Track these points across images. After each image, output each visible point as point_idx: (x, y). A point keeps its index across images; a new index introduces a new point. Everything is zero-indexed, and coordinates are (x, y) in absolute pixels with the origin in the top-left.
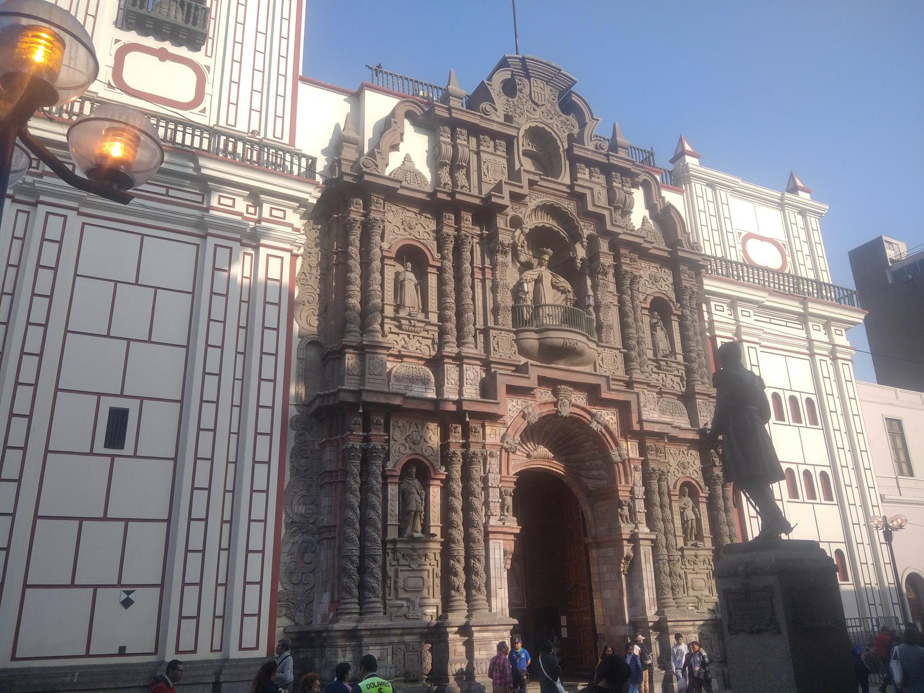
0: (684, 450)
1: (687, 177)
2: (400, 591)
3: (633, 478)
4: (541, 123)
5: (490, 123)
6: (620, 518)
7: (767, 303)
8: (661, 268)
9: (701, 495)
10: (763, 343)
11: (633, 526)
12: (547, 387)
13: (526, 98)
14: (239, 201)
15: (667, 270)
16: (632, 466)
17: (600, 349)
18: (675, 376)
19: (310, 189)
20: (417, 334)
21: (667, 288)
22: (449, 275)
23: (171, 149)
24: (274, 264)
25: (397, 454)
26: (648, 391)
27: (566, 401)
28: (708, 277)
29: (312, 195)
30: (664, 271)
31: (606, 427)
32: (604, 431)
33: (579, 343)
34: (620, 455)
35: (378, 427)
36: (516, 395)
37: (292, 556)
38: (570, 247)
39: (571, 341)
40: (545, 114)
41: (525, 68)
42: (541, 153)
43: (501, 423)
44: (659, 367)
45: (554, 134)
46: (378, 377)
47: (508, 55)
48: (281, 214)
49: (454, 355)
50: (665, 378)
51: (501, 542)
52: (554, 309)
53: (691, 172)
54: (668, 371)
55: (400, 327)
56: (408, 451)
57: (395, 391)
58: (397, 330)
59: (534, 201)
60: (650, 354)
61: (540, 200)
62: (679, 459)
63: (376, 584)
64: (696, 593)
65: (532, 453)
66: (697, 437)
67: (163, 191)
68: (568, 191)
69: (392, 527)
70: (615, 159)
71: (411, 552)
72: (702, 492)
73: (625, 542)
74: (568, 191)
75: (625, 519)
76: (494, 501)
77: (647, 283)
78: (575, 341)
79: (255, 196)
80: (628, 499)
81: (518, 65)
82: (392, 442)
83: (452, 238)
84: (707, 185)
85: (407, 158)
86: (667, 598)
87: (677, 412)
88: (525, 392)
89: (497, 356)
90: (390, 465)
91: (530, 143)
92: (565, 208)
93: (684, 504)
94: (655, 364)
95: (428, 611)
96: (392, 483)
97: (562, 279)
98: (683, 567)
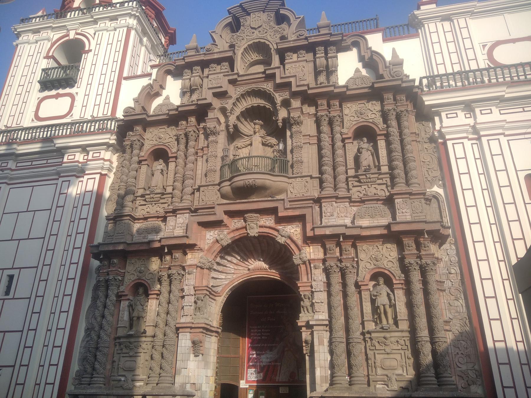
0: (378, 245)
1: (421, 22)
2: (120, 370)
3: (313, 276)
4: (257, 39)
5: (212, 55)
6: (302, 309)
7: (507, 96)
8: (368, 102)
9: (395, 282)
10: (507, 133)
11: (312, 314)
12: (238, 217)
13: (248, 28)
14: (78, 154)
15: (374, 102)
16: (312, 265)
17: (290, 181)
18: (379, 184)
19: (108, 136)
20: (157, 202)
21: (373, 116)
22: (180, 161)
23: (42, 140)
24: (91, 182)
25: (129, 281)
26: (336, 202)
27: (252, 224)
28: (425, 94)
29: (112, 139)
30: (372, 104)
31: (290, 238)
32: (289, 241)
33: (257, 180)
34: (300, 259)
35: (114, 265)
36: (214, 228)
37: (86, 349)
38: (275, 112)
39: (248, 180)
40: (262, 31)
41: (244, 10)
42: (266, 58)
43: (198, 250)
44: (359, 181)
45: (267, 42)
46: (122, 234)
47: (229, 8)
48: (98, 155)
49: (171, 210)
50: (367, 188)
51: (188, 334)
52: (263, 160)
53: (419, 17)
54: (369, 182)
55: (145, 200)
56: (136, 277)
57: (137, 241)
58: (144, 203)
59: (234, 92)
60: (351, 172)
61: (242, 90)
62: (371, 253)
63: (98, 366)
64: (385, 372)
65: (250, 267)
66: (385, 232)
67: (45, 162)
68: (264, 76)
69: (120, 328)
70: (313, 38)
71: (128, 343)
72: (396, 280)
73: (304, 329)
74: (264, 76)
75: (306, 310)
76: (186, 305)
77: (353, 118)
78: (253, 180)
79: (84, 149)
80: (308, 294)
81: (240, 10)
82: (126, 274)
83: (183, 136)
84: (442, 20)
85: (167, 98)
86: (337, 376)
87: (377, 214)
88: (217, 224)
89: (204, 204)
90: (122, 288)
91: (257, 55)
92: (263, 88)
93: (377, 292)
94: (357, 179)
95: (138, 384)
96: (123, 300)
97: (269, 138)
98: (373, 348)
